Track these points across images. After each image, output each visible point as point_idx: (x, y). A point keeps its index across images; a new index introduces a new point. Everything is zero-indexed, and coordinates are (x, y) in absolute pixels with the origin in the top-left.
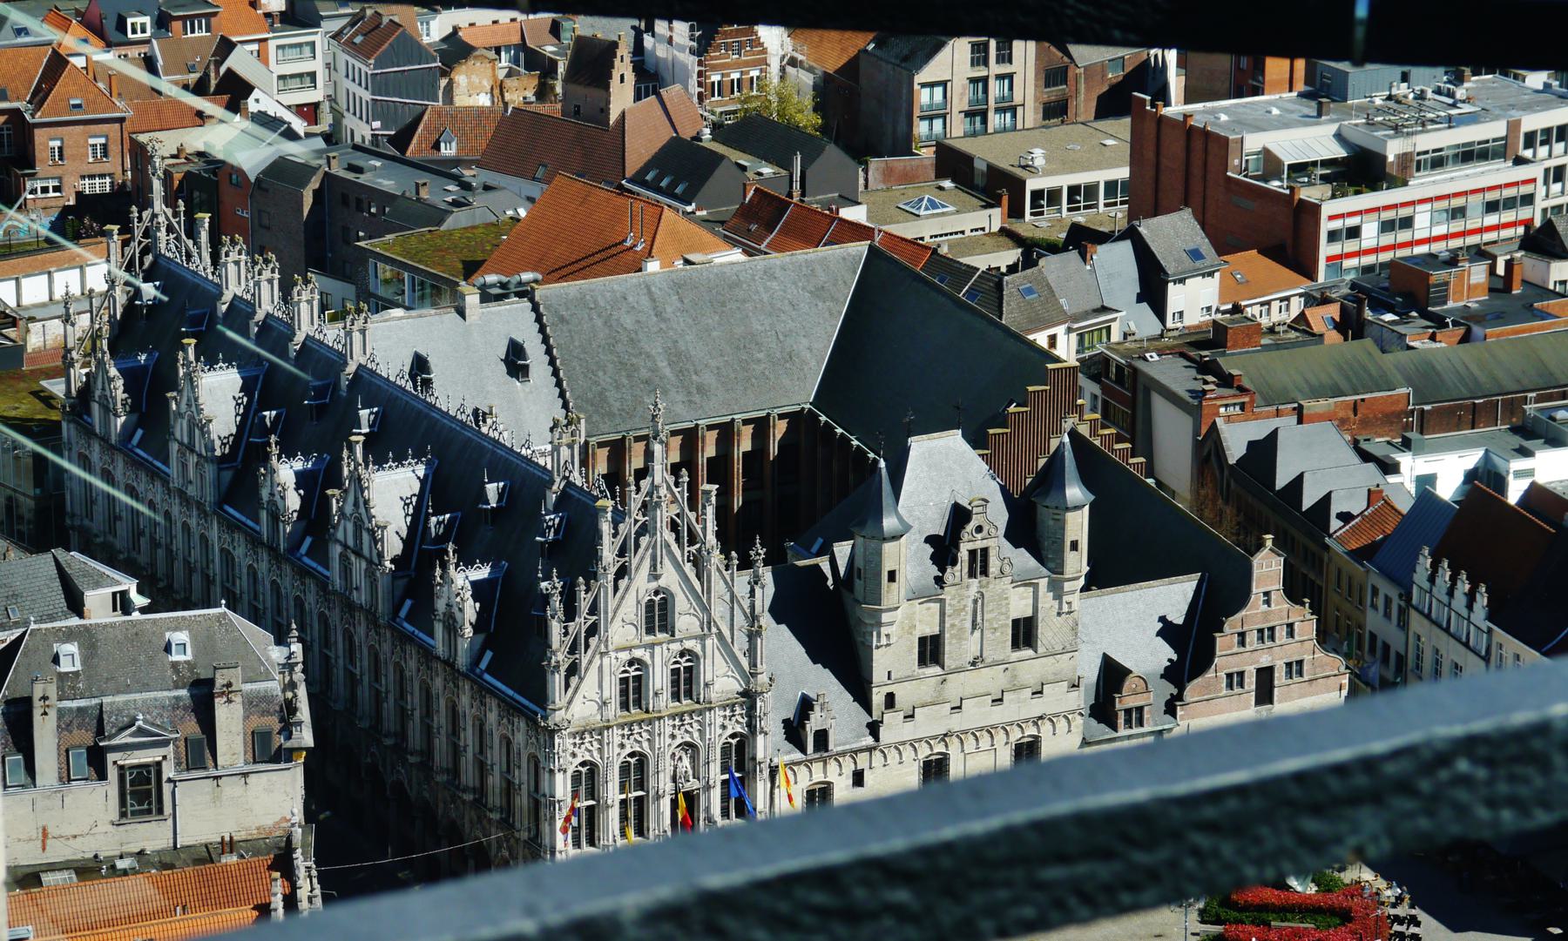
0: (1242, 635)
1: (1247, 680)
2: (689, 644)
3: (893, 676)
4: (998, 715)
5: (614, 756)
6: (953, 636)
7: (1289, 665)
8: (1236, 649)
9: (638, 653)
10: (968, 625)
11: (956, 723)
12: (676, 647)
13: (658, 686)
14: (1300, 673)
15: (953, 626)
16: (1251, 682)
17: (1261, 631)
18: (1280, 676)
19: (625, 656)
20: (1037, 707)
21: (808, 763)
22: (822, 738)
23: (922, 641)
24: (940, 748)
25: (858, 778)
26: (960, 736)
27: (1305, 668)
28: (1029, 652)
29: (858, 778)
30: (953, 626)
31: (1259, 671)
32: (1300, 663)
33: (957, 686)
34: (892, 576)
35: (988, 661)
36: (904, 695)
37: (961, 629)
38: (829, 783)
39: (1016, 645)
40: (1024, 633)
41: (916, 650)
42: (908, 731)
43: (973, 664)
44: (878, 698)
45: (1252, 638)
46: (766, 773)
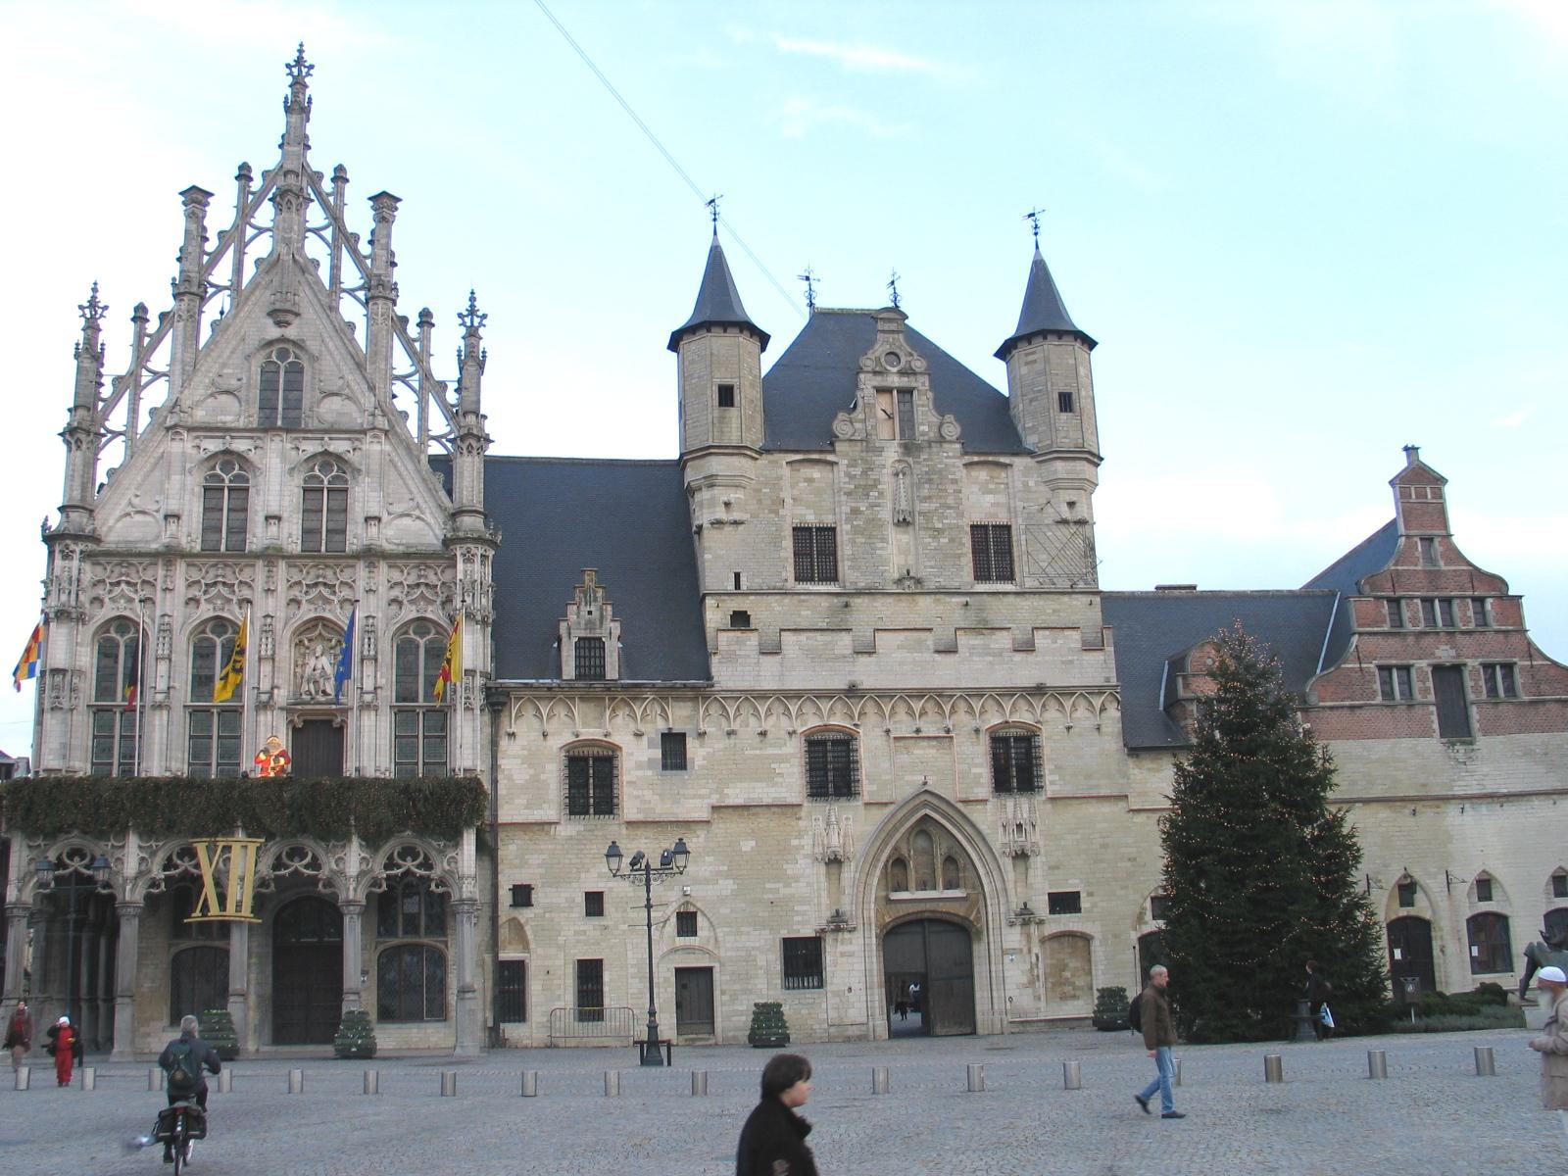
0: (1395, 602)
1: (1416, 685)
2: (339, 446)
3: (744, 586)
4: (946, 673)
5: (173, 609)
6: (856, 530)
7: (1489, 667)
8: (1386, 628)
9: (240, 445)
10: (886, 514)
11: (868, 674)
12: (311, 447)
13: (274, 510)
14: (1511, 690)
15: (855, 511)
16: (1424, 687)
17: (1424, 600)
18: (1474, 685)
19: (213, 446)
20: (1025, 672)
21: (562, 694)
22: (592, 649)
23: (801, 532)
24: (838, 720)
25: (674, 750)
26: (883, 695)
27: (1519, 679)
28: (1008, 587)
29: (674, 750)
30: (855, 511)
31: (1438, 669)
32: (1508, 668)
33: (867, 613)
34: (726, 396)
35: (931, 585)
36: (762, 612)
37: (874, 523)
38: (615, 748)
39: (982, 574)
40: (993, 551)
41: (788, 544)
42: (768, 675)
43: (899, 581)
44: (715, 615)
45: (1413, 613)
46: (478, 700)
